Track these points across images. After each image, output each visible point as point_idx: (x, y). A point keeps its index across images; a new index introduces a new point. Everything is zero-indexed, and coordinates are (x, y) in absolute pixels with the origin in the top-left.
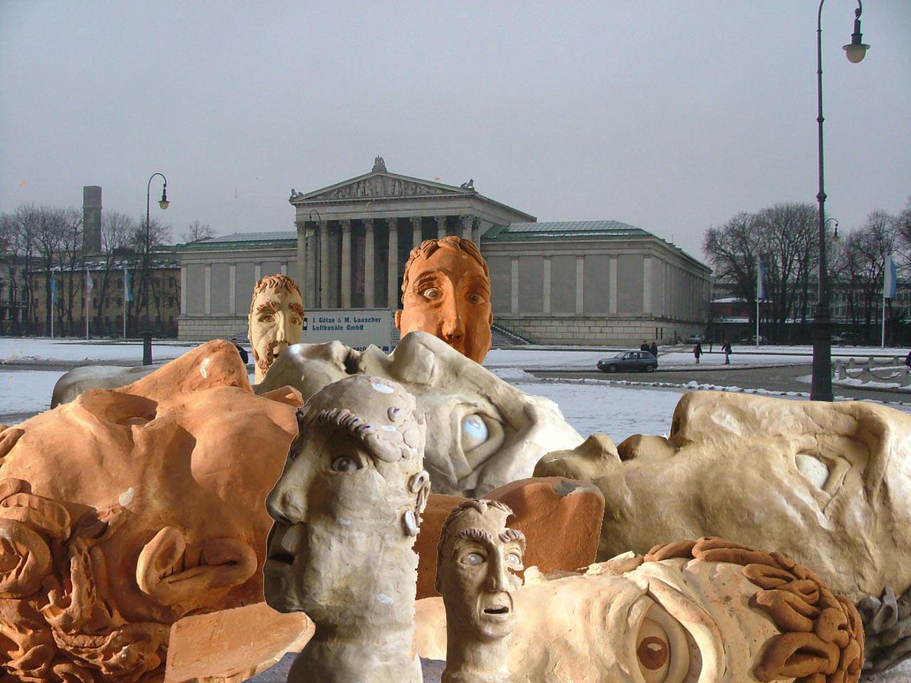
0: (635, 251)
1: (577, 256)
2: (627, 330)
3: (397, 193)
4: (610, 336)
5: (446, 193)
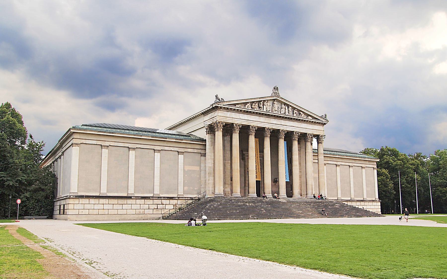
0: (371, 166)
3: (287, 113)
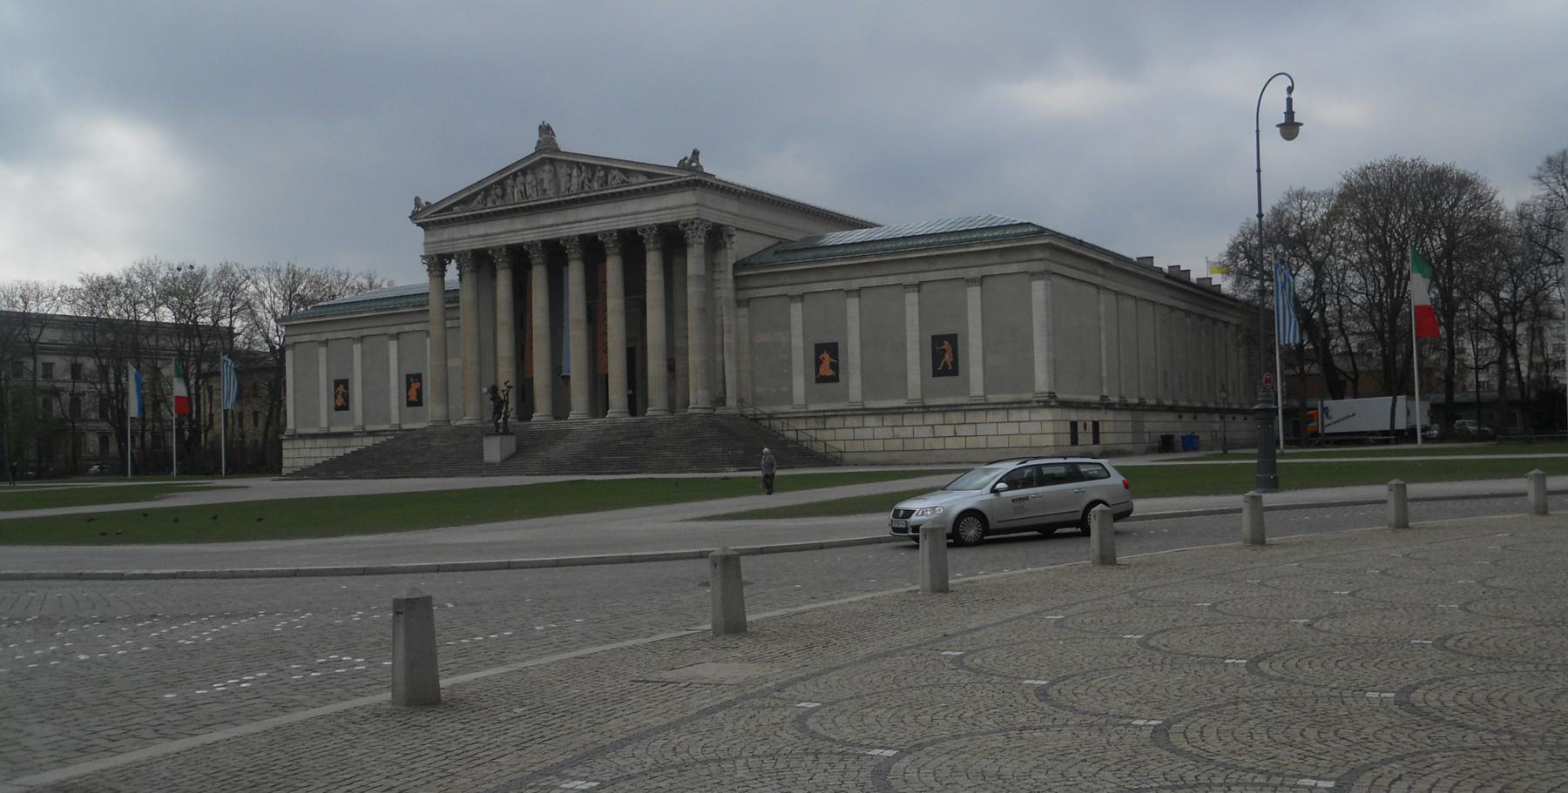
0: (1014, 268)
1: (906, 286)
2: (1003, 429)
3: (574, 188)
4: (971, 443)
5: (655, 182)
